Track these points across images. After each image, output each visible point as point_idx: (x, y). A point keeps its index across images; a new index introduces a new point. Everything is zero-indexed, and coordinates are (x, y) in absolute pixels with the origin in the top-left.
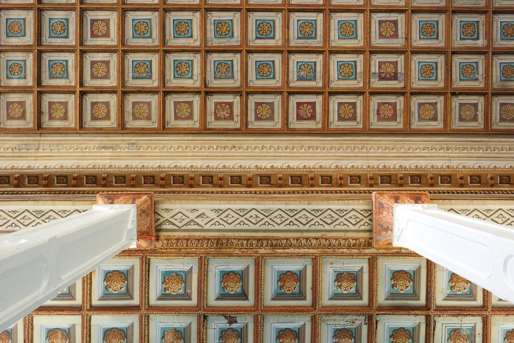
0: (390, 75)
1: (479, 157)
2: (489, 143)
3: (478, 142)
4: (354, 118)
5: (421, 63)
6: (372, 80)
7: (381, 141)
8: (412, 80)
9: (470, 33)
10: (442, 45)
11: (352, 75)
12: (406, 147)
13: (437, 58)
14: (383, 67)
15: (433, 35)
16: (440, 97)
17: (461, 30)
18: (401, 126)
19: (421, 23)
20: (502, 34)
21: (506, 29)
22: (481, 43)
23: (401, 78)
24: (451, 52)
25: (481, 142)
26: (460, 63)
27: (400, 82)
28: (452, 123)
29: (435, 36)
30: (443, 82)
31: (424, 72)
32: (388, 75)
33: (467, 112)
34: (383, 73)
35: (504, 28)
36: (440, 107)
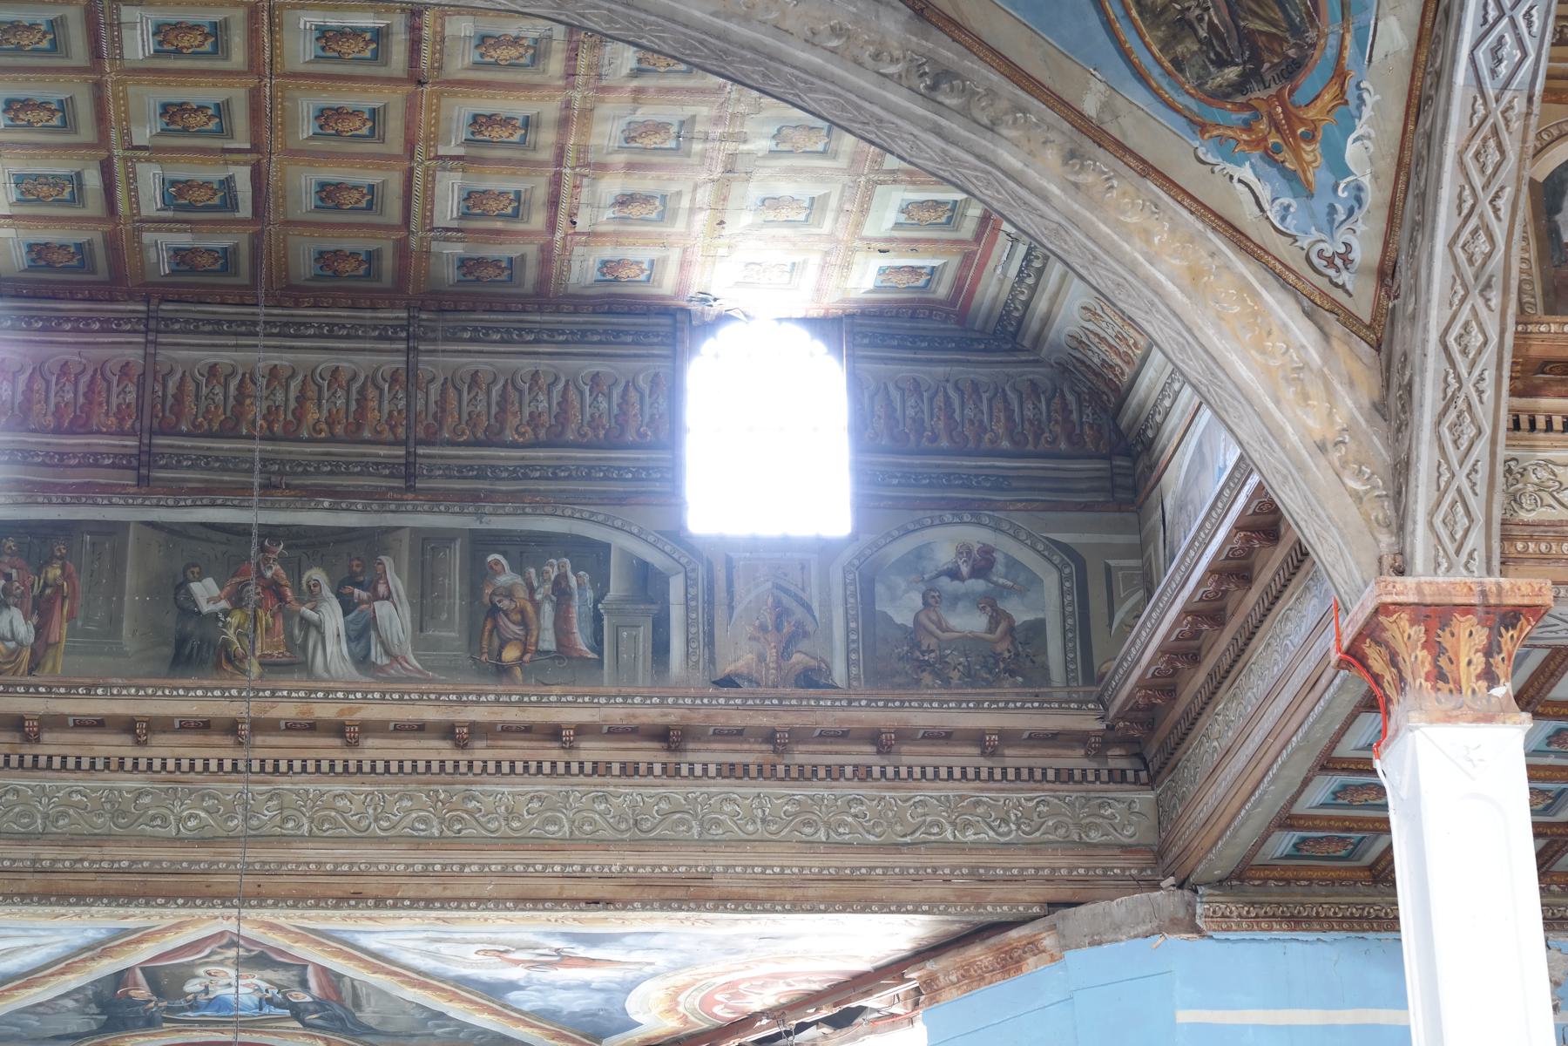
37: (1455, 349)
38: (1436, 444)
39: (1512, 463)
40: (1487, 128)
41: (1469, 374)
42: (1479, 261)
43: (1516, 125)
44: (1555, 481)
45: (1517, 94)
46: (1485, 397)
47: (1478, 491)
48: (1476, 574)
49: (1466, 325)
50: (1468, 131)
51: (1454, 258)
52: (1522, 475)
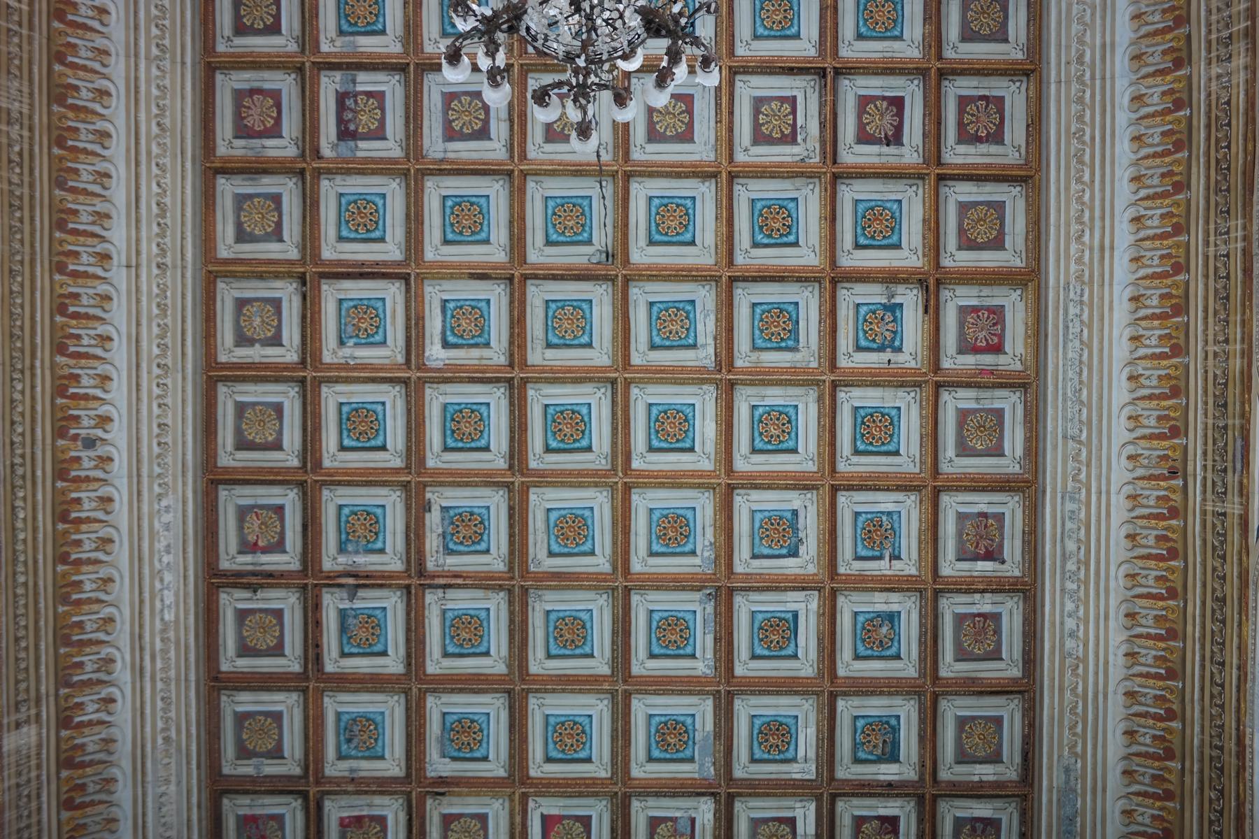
0: (350, 121)
1: (137, 341)
2: (180, 376)
3: (183, 345)
4: (241, 29)
5: (382, 201)
6: (338, 75)
7: (183, 98)
8: (338, 179)
9: (459, 326)
10: (429, 255)
11: (351, 24)
12: (167, 161)
13: (396, 242)
14: (370, 103)
15: (454, 231)
16: (296, 251)
17: (468, 303)
18: (222, 150)
19: (483, 201)
20: (457, 407)
21: (470, 417)
22: (435, 353)
23: (345, 149)
24: (409, 274)
25: (183, 354)
26: (383, 300)
27: (334, 147)
28: (231, 280)
29: (450, 236)
30: (335, 256)
31: (358, 208)
32: (350, 116)
33: (259, 319)
34: (356, 102)
35: (473, 412)
36: (271, 250)
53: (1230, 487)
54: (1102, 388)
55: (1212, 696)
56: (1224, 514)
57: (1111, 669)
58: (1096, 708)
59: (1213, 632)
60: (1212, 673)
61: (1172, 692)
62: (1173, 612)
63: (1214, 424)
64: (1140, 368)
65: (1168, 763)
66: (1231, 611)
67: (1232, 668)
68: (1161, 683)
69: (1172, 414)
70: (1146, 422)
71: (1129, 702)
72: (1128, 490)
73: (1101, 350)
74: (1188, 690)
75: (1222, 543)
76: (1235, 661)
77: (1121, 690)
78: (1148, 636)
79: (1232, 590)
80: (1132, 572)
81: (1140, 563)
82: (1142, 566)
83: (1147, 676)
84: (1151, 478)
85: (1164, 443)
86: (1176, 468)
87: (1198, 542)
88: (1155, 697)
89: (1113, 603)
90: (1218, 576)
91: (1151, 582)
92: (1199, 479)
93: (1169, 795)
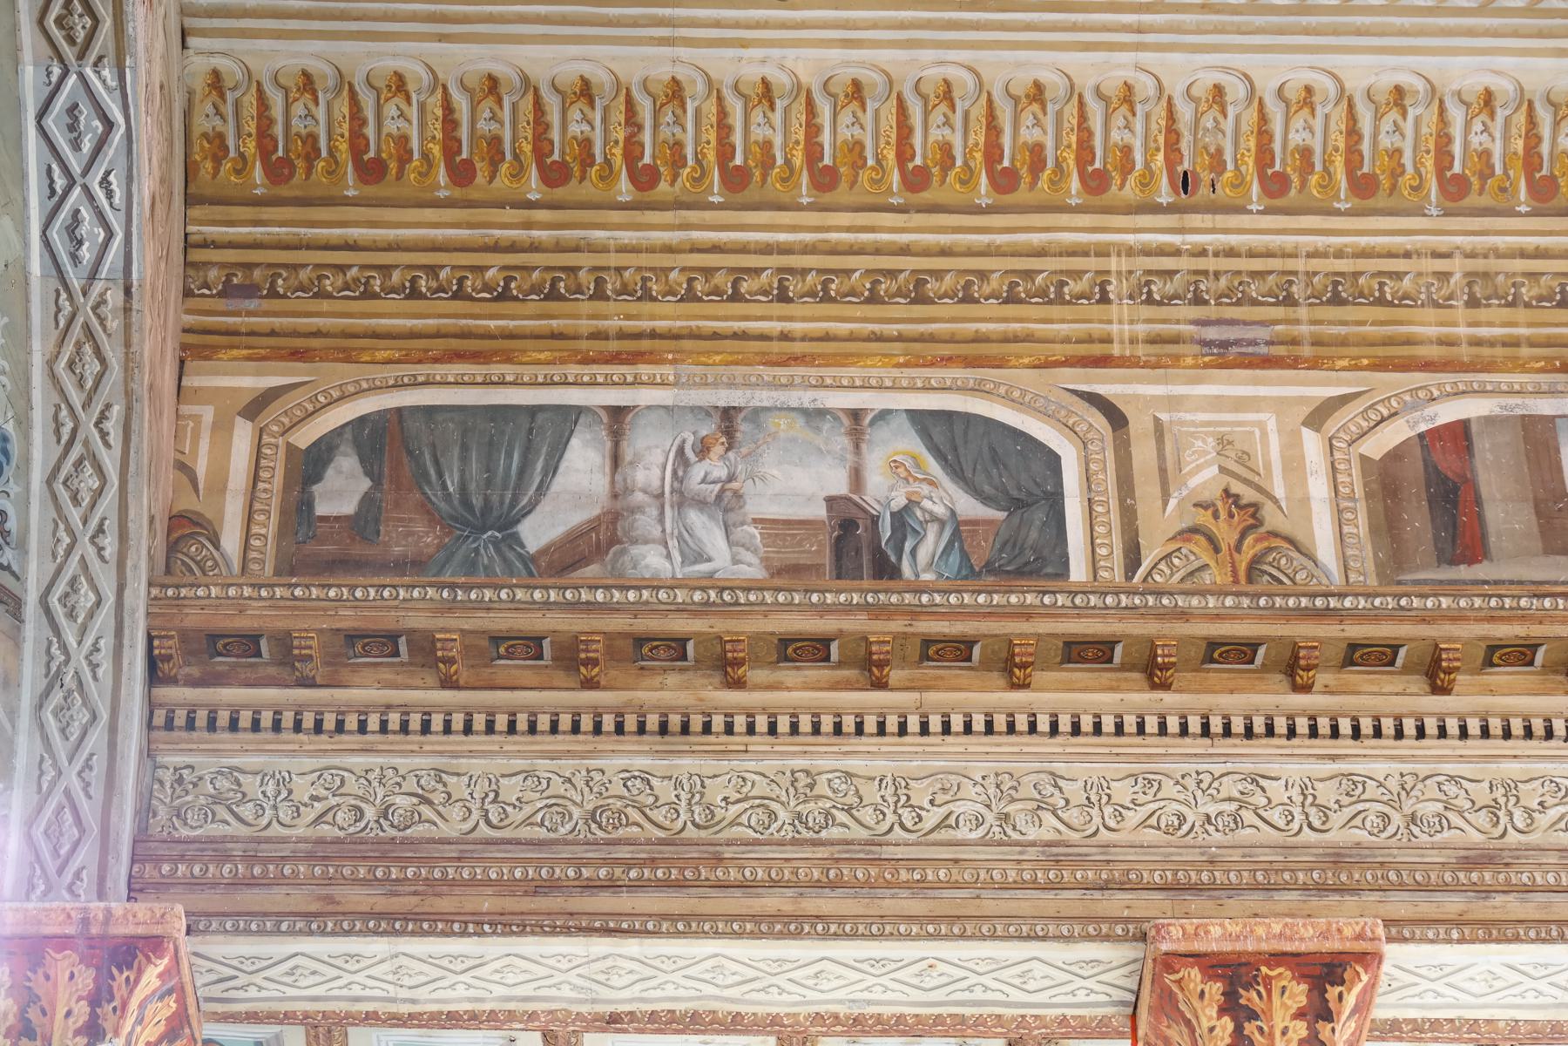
37: (59, 611)
38: (38, 735)
39: (185, 772)
40: (77, 330)
41: (79, 643)
42: (87, 500)
43: (115, 324)
44: (236, 792)
45: (110, 284)
46: (100, 672)
47: (92, 793)
48: (83, 898)
49: (73, 582)
50: (55, 335)
51: (54, 497)
52: (195, 785)
53: (1164, 312)
54: (1382, 34)
55: (708, 272)
56: (1104, 299)
57: (730, 53)
58: (635, 23)
59: (848, 272)
60: (758, 271)
61: (696, 181)
62: (873, 181)
63: (1295, 273)
64: (1419, 111)
65: (534, 172)
66: (900, 317)
67: (780, 319)
68: (711, 156)
69: (1314, 179)
70: (1298, 122)
71: (658, 90)
72: (1146, 86)
73: (1471, 32)
74: (708, 216)
75: (1043, 293)
76: (798, 327)
77: (682, 73)
78: (813, 129)
79: (945, 319)
80: (956, 94)
81: (978, 111)
82: (972, 116)
83: (724, 128)
84: (1172, 134)
85: (1251, 162)
86: (1196, 187)
87: (1036, 239)
88: (678, 145)
89: (884, 56)
90: (969, 284)
91: (936, 134)
92: (1176, 239)
93: (462, 173)
